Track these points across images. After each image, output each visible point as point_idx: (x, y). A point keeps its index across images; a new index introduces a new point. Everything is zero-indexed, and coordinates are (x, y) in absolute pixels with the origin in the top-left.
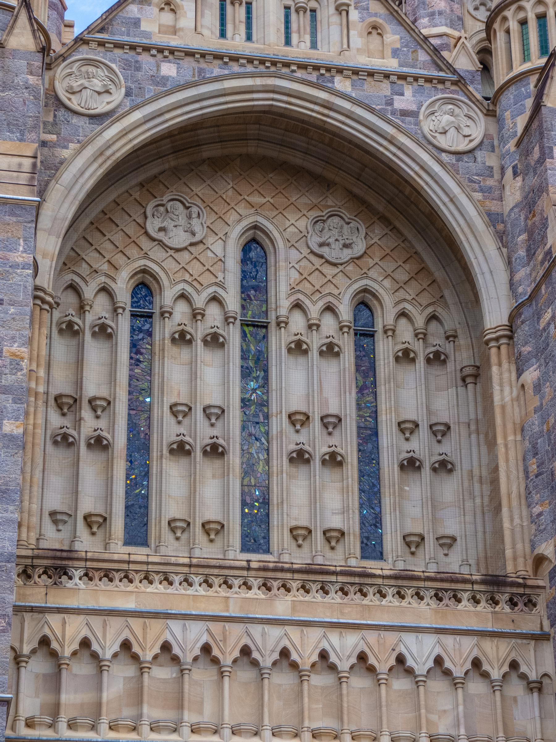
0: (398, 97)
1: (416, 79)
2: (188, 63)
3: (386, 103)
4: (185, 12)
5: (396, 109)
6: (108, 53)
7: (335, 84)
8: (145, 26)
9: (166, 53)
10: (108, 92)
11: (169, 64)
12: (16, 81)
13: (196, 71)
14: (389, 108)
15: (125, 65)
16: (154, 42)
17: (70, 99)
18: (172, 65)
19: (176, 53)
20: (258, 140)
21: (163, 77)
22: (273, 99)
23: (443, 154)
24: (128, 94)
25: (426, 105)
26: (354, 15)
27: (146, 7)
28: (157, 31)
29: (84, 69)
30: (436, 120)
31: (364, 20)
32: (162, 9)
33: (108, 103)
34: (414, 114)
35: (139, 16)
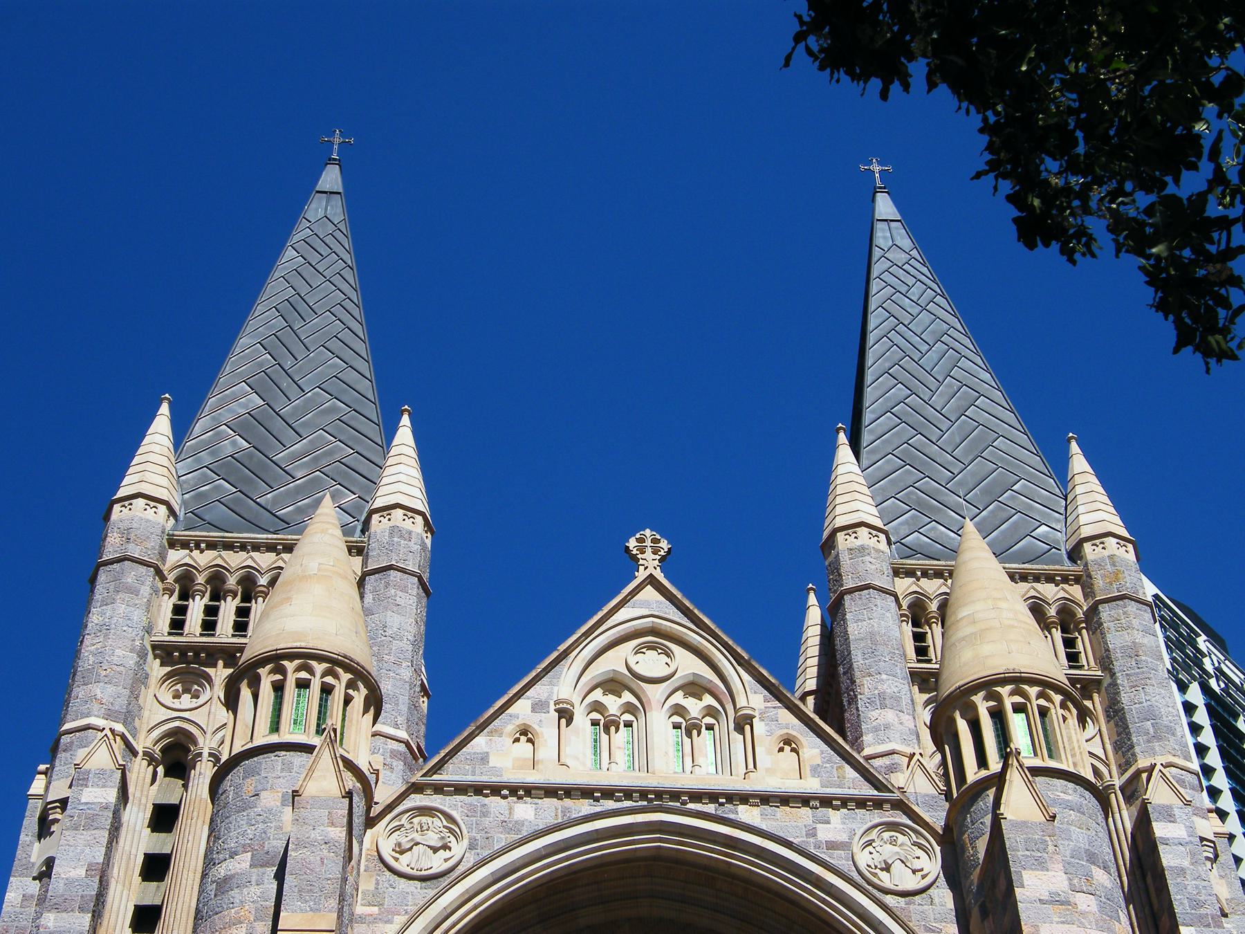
2: (550, 803)
4: (545, 741)
6: (448, 798)
8: (494, 761)
9: (521, 792)
10: (446, 847)
12: (313, 835)
13: (559, 811)
14: (812, 840)
16: (506, 780)
17: (397, 859)
18: (528, 806)
21: (516, 822)
22: (660, 840)
23: (889, 896)
24: (472, 847)
25: (859, 833)
29: (416, 820)
33: (446, 860)
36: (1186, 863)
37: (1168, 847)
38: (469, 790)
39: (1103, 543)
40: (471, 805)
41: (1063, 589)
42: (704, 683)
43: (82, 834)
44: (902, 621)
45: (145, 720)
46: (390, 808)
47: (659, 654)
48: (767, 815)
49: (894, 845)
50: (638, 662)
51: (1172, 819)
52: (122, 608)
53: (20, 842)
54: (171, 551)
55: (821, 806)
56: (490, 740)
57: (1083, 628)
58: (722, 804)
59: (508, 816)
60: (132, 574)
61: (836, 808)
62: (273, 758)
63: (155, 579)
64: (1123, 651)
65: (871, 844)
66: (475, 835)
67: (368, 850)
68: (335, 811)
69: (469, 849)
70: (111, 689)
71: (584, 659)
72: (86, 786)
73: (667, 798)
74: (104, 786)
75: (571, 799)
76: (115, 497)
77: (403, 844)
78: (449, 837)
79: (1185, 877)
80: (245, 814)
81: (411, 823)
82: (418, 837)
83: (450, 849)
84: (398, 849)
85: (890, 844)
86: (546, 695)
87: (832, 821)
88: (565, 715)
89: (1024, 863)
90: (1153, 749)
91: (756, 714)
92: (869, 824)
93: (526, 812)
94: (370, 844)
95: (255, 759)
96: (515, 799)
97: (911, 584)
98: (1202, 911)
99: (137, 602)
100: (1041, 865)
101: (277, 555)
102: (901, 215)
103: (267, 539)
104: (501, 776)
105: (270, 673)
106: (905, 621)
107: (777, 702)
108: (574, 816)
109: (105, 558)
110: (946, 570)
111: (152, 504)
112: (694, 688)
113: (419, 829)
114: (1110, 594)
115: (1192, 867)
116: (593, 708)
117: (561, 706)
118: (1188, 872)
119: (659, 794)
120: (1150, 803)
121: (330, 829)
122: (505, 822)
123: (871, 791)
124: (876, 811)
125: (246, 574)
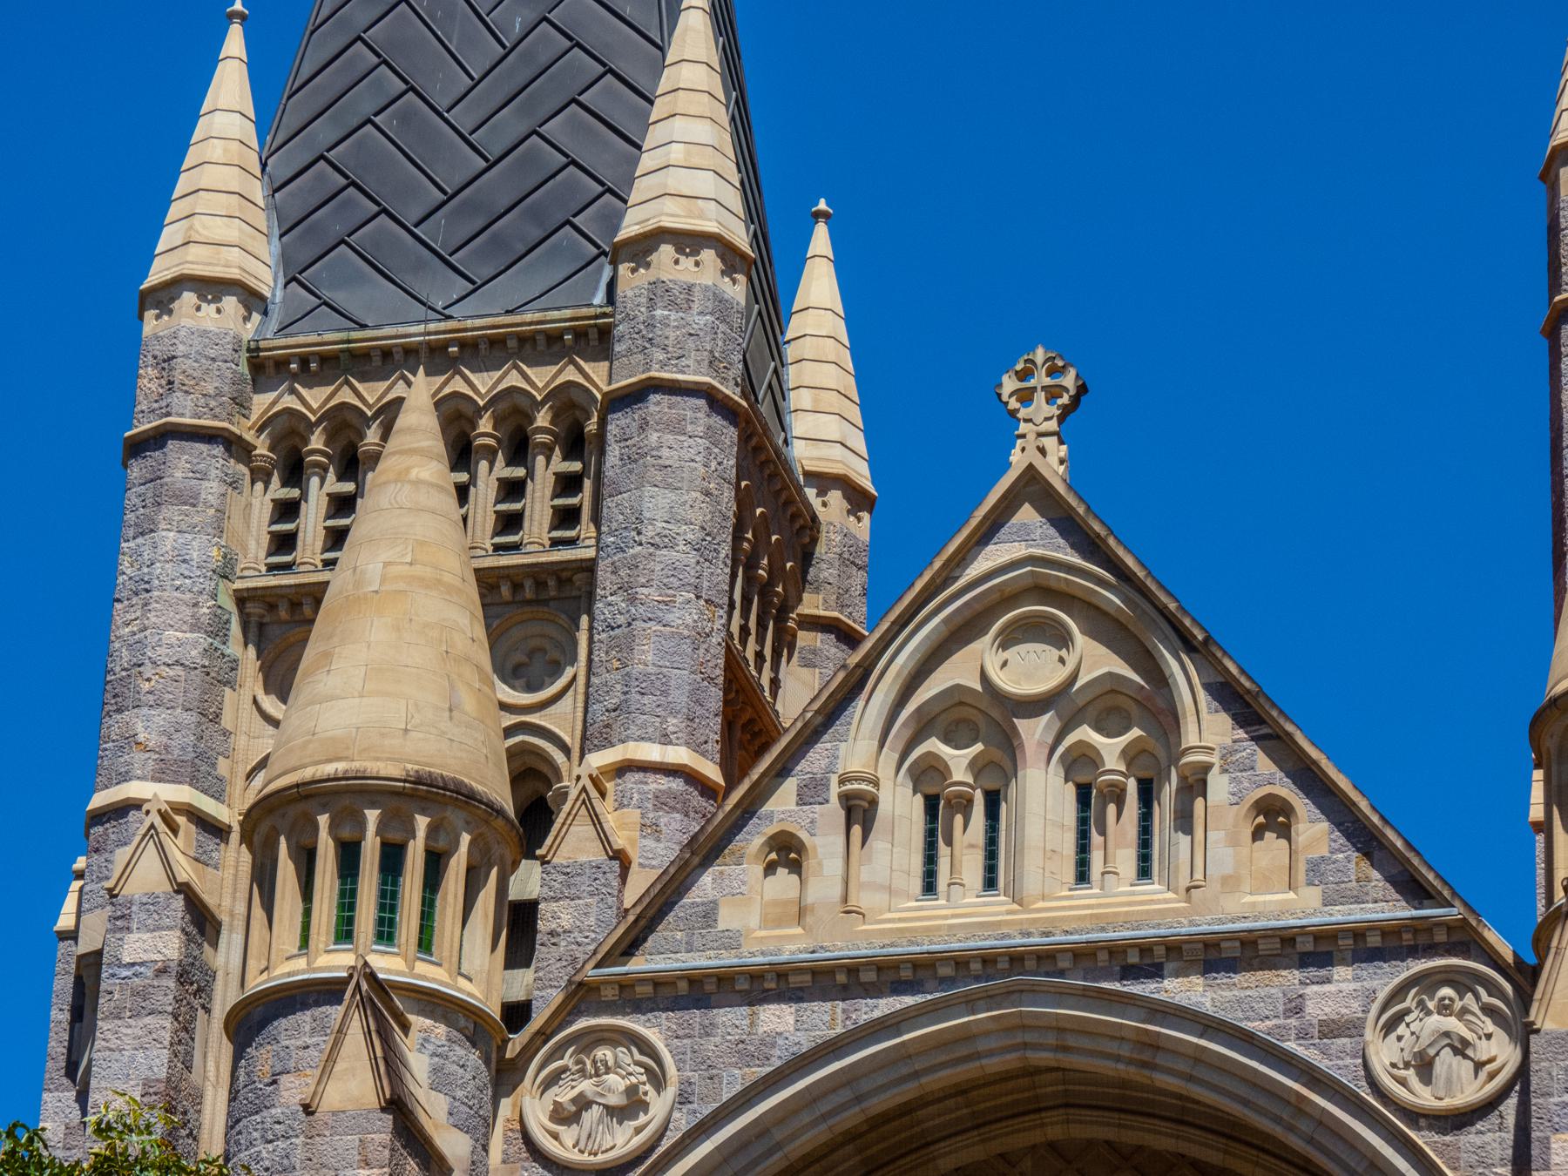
0: (1315, 988)
3: (1285, 1011)
4: (820, 864)
8: (727, 919)
14: (1293, 1022)
17: (555, 1136)
20: (1067, 1105)
24: (683, 1099)
25: (1382, 996)
26: (1219, 786)
30: (1407, 1034)
33: (638, 1131)
34: (1351, 1028)
45: (239, 756)
52: (168, 539)
60: (180, 461)
69: (680, 1103)
70: (161, 718)
74: (158, 928)
80: (258, 1118)
82: (586, 1086)
85: (1439, 1013)
86: (824, 763)
91: (1214, 759)
99: (196, 519)
117: (849, 787)
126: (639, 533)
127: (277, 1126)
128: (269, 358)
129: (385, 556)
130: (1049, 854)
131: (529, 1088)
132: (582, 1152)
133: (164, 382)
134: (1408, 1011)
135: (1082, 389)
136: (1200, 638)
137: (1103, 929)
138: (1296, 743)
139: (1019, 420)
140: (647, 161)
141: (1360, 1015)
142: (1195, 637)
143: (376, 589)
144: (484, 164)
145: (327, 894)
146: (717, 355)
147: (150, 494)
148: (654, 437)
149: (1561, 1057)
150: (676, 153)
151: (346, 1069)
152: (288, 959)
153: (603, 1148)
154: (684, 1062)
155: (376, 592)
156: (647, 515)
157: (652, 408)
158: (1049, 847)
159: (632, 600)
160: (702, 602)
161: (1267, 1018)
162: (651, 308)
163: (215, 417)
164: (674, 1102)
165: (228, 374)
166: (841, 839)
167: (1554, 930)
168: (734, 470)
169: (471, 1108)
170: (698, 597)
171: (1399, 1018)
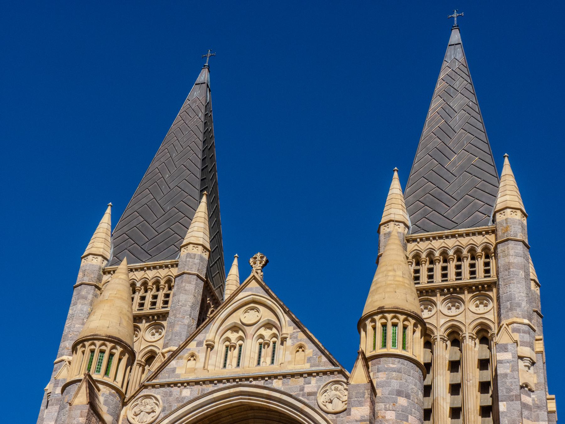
0: (307, 385)
1: (318, 373)
3: (300, 390)
4: (200, 359)
5: (305, 393)
6: (157, 389)
7: (273, 384)
8: (178, 371)
9: (185, 384)
10: (153, 411)
11: (186, 390)
13: (200, 391)
14: (301, 393)
15: (164, 394)
18: (188, 390)
19: (190, 383)
21: (182, 397)
22: (241, 399)
23: (329, 415)
24: (163, 410)
25: (322, 387)
26: (289, 342)
27: (180, 361)
28: (184, 372)
29: (143, 401)
30: (327, 395)
31: (294, 344)
32: (190, 360)
33: (153, 417)
35: (175, 366)
36: (508, 371)
37: (502, 364)
38: (165, 386)
39: (504, 212)
40: (166, 392)
41: (486, 238)
42: (272, 323)
43: (55, 407)
44: (409, 265)
46: (133, 396)
47: (255, 312)
48: (285, 383)
49: (336, 391)
50: (245, 317)
51: (506, 350)
52: (79, 306)
53: (41, 410)
54: (104, 276)
55: (308, 376)
56: (178, 362)
57: (493, 256)
58: (267, 380)
59: (179, 395)
61: (315, 376)
62: (75, 386)
63: (95, 291)
64: (504, 267)
65: (326, 392)
66: (165, 405)
67: (124, 416)
68: (83, 410)
71: (221, 319)
72: (58, 386)
73: (244, 380)
75: (206, 385)
76: (82, 256)
77: (136, 412)
78: (155, 407)
79: (506, 378)
80: (63, 411)
81: (141, 402)
82: (142, 408)
83: (155, 412)
84: (135, 414)
85: (335, 390)
86: (203, 338)
87: (312, 383)
88: (210, 347)
89: (353, 404)
90: (508, 315)
92: (328, 382)
93: (187, 393)
94: (124, 413)
95: (70, 387)
96: (183, 387)
97: (415, 246)
98: (512, 393)
99: (86, 302)
100: (360, 404)
101: (145, 272)
102: (462, 40)
103: (140, 265)
104: (179, 377)
105: (81, 347)
106: (410, 264)
107: (299, 329)
108: (206, 392)
109: (77, 284)
110: (431, 236)
111: (96, 257)
112: (269, 325)
113: (144, 405)
114: (503, 238)
115: (511, 373)
116: (226, 340)
117: (208, 343)
118: (509, 375)
119: (241, 379)
120: (498, 344)
121: (80, 418)
122: (178, 398)
123: (331, 367)
124: (331, 376)
125: (132, 282)
126: (179, 303)
127: (67, 412)
128: (107, 271)
129: (110, 292)
130: (251, 358)
131: (129, 408)
132: (139, 422)
133: (83, 275)
134: (327, 390)
135: (267, 261)
136: (287, 310)
137: (261, 373)
138: (306, 332)
139: (253, 267)
140: (189, 231)
141: (317, 391)
142: (286, 310)
143: (107, 298)
144: (158, 234)
145: (86, 361)
146: (200, 268)
147: (77, 297)
148: (184, 284)
149: (355, 390)
150: (195, 229)
151: (80, 396)
152: (75, 376)
153: (144, 422)
154: (165, 403)
155: (107, 299)
156: (180, 300)
157: (184, 278)
158: (251, 356)
159: (175, 317)
160: (191, 318)
161: (296, 392)
162: (186, 258)
163: (93, 282)
164: (161, 411)
165: (97, 273)
166: (205, 354)
167: (355, 363)
168: (202, 293)
169: (113, 410)
170: (190, 317)
171: (326, 391)
